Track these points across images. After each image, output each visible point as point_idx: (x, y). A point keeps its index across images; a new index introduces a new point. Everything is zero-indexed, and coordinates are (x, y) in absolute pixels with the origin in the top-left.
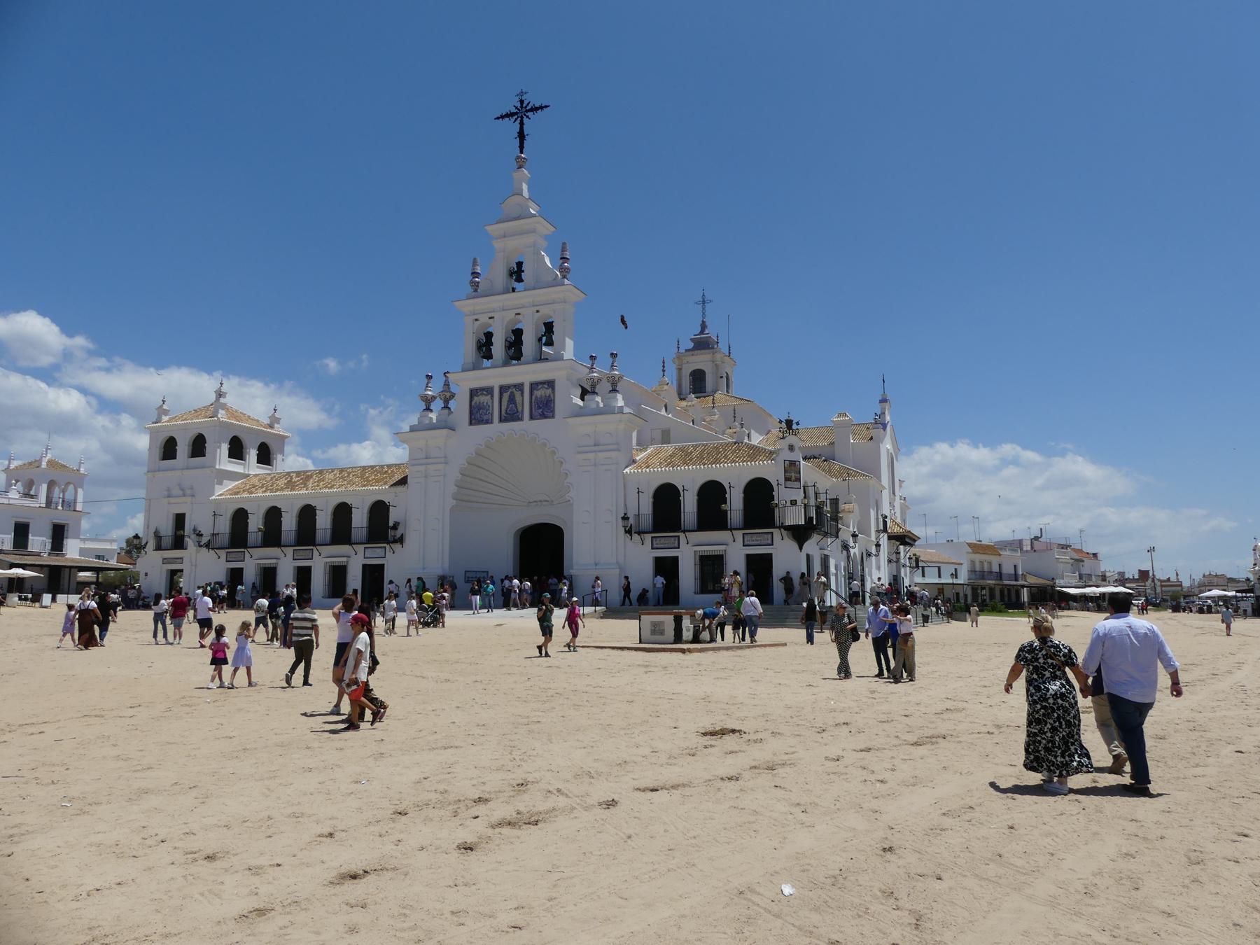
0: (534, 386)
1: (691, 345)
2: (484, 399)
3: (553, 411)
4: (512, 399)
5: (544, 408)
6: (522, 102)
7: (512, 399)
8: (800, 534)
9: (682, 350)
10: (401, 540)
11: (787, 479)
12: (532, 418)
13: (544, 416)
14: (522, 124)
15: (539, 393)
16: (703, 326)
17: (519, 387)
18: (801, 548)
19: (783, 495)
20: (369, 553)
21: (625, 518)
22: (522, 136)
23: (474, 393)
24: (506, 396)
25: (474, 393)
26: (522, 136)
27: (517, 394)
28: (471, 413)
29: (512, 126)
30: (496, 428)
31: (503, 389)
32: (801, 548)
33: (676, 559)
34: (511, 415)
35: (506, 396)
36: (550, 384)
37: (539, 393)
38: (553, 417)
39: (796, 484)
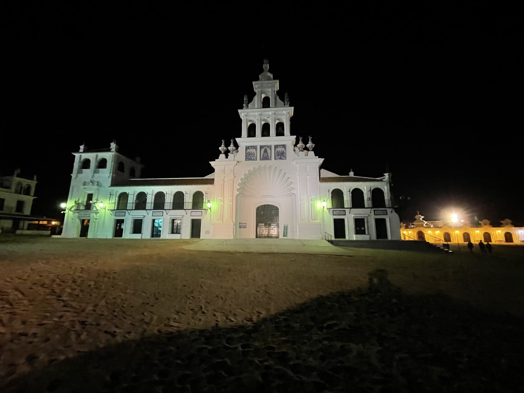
0: (276, 147)
3: (285, 157)
4: (266, 151)
5: (281, 155)
7: (266, 151)
12: (275, 159)
13: (280, 158)
15: (279, 149)
17: (270, 147)
20: (193, 214)
23: (247, 148)
24: (263, 150)
25: (247, 148)
27: (268, 150)
28: (246, 156)
30: (259, 163)
31: (261, 147)
33: (343, 220)
34: (265, 157)
35: (263, 150)
36: (284, 146)
38: (285, 159)
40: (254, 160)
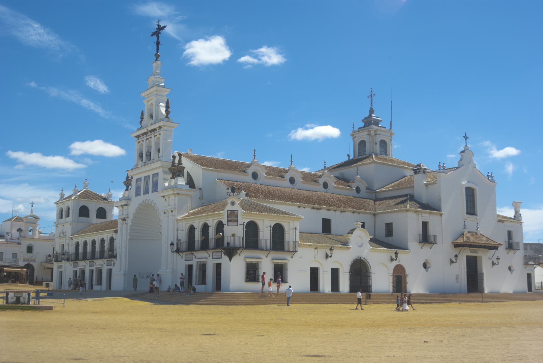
0: (154, 175)
1: (363, 124)
2: (139, 183)
4: (147, 184)
6: (158, 25)
8: (231, 252)
9: (356, 129)
10: (115, 257)
11: (228, 221)
14: (158, 37)
16: (372, 111)
17: (149, 176)
18: (230, 259)
19: (228, 230)
21: (172, 244)
22: (158, 44)
26: (158, 44)
29: (155, 38)
32: (230, 259)
36: (157, 174)
37: (155, 179)
39: (235, 224)
40: (140, 195)
